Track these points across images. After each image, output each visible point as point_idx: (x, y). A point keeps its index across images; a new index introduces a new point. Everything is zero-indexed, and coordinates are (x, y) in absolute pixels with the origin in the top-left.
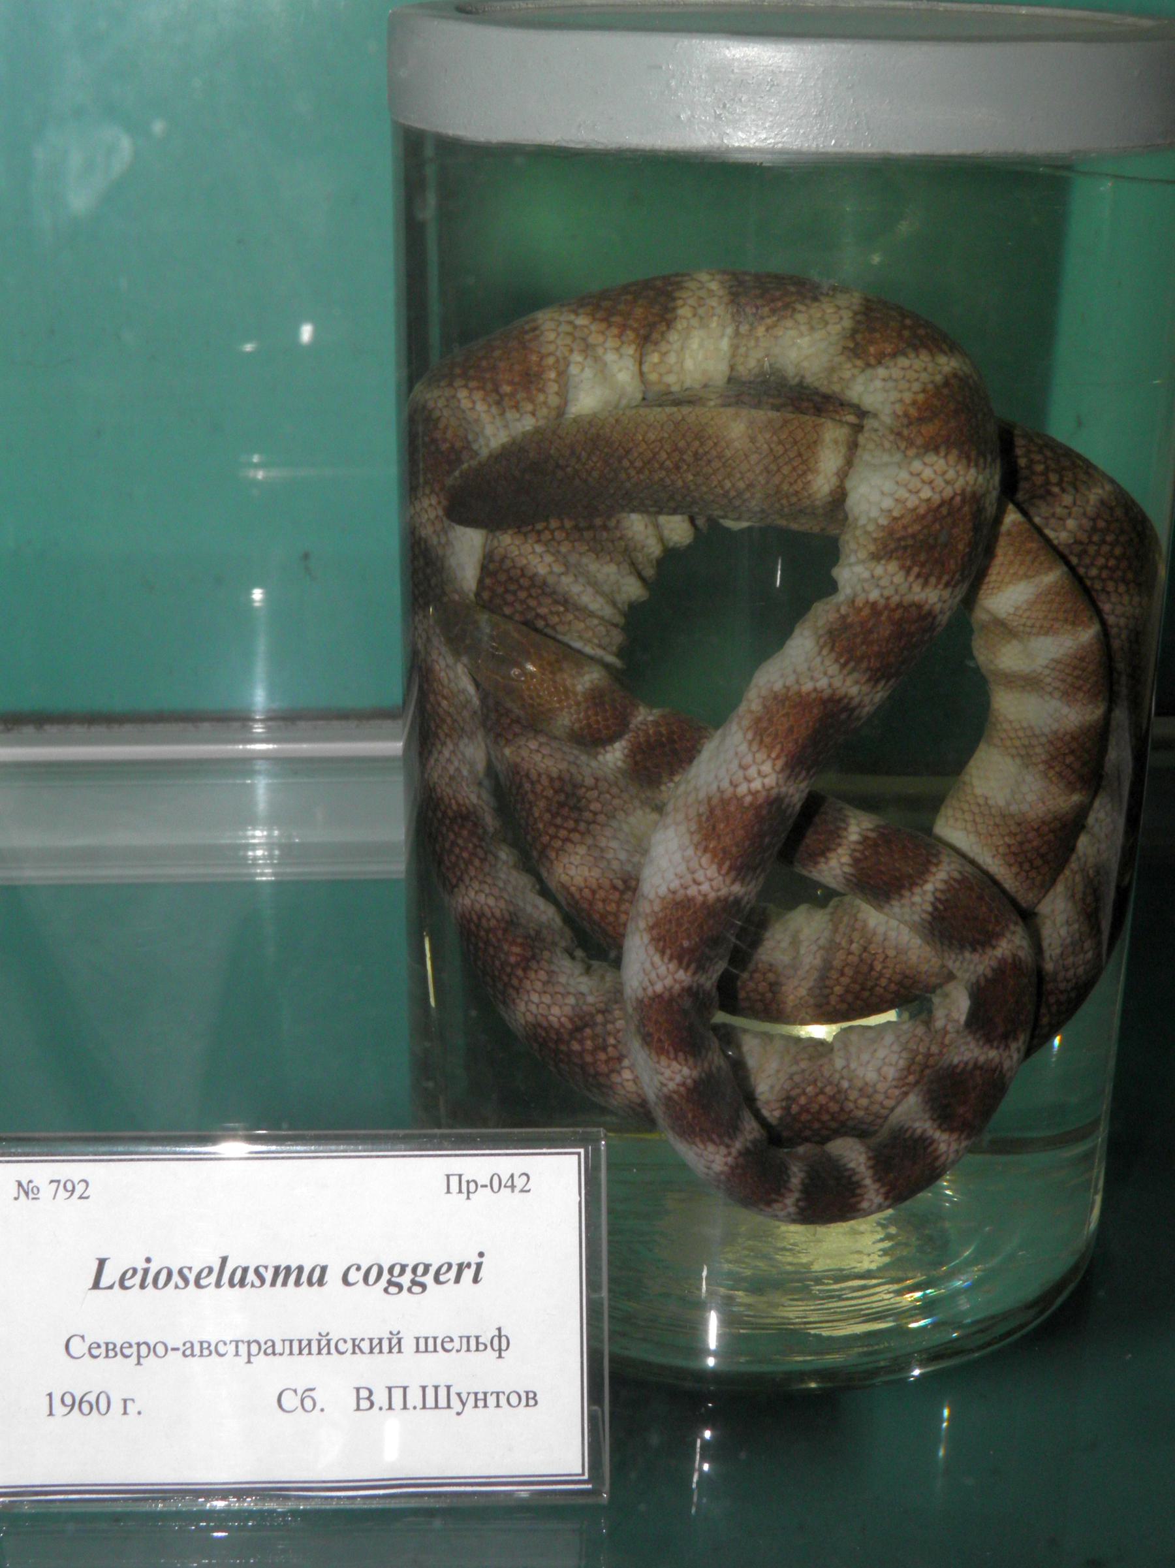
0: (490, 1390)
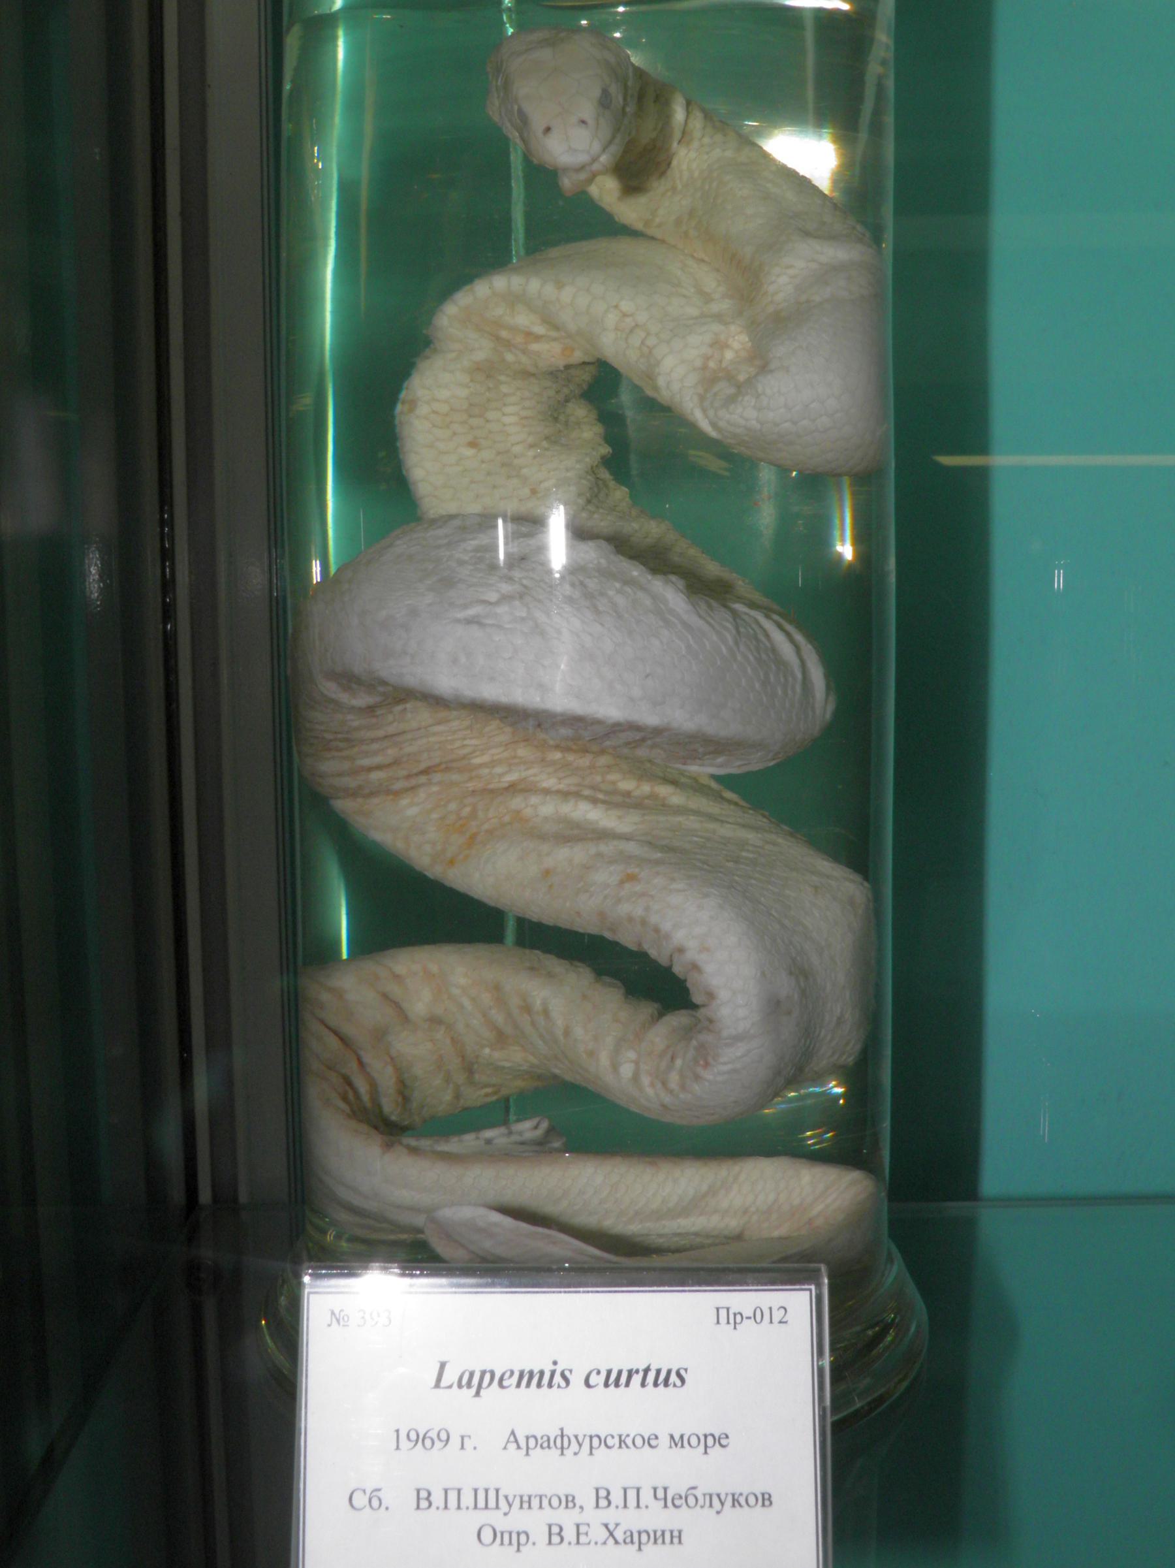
0: (534, 1493)
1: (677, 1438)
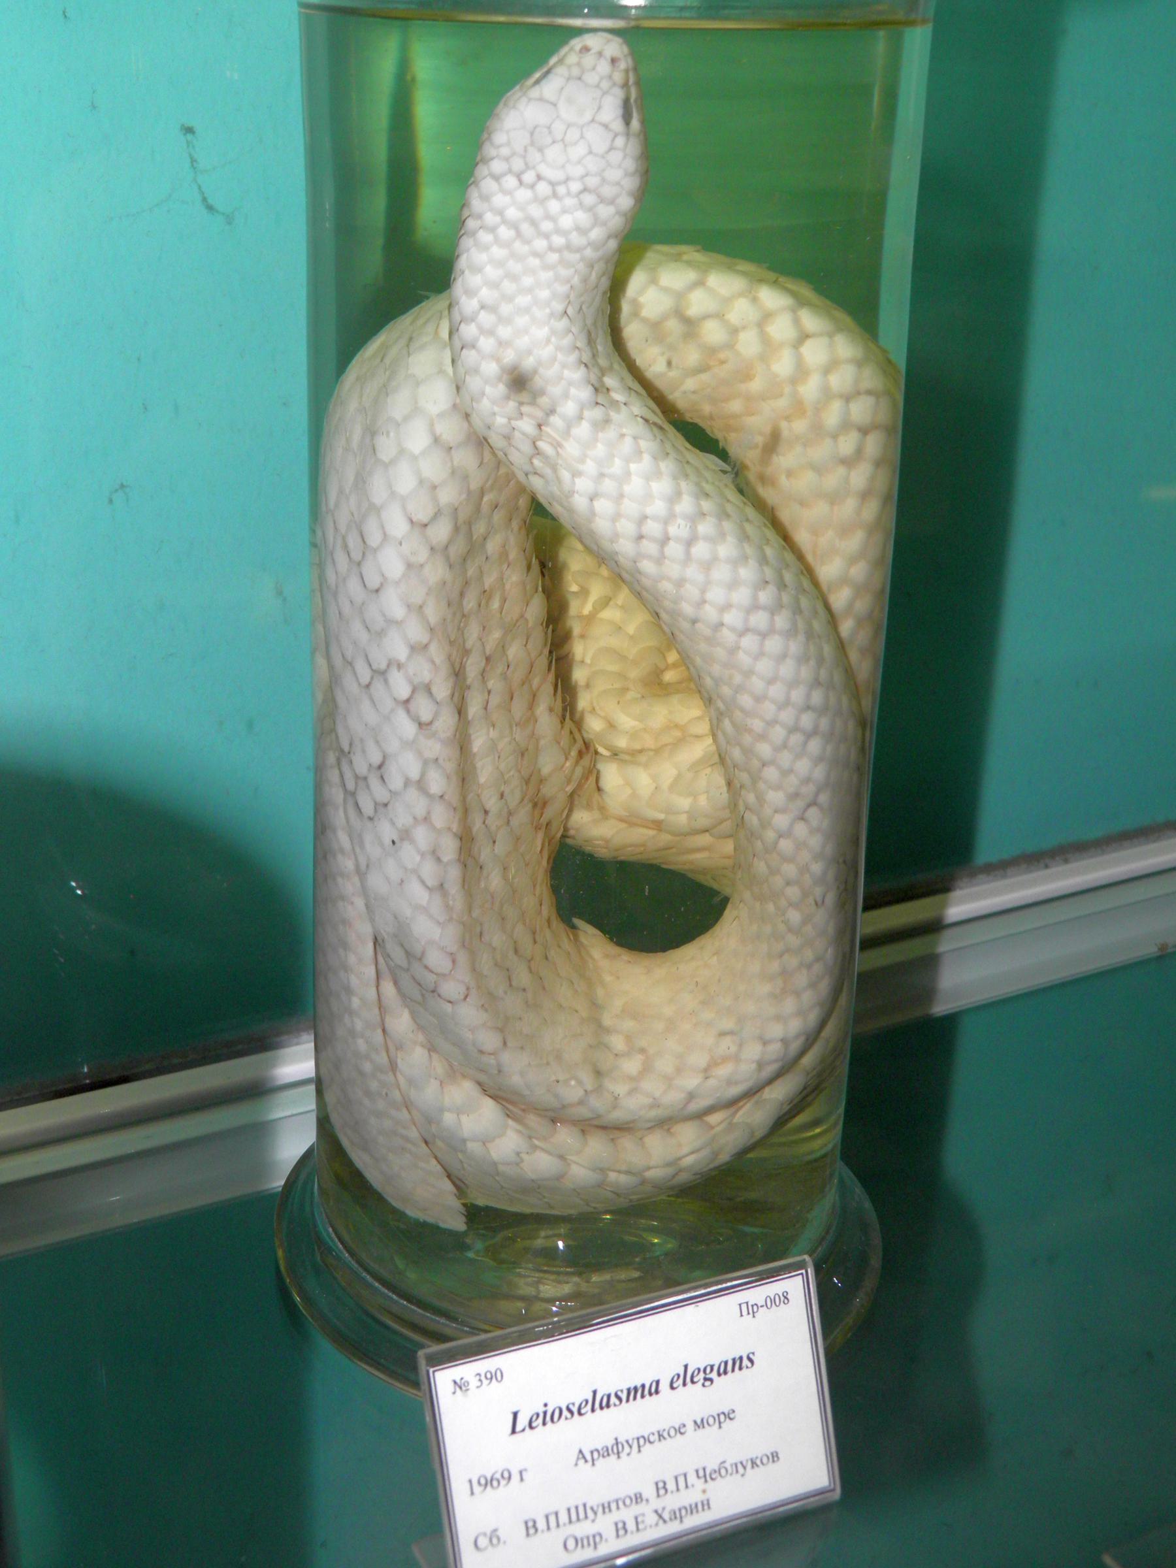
1: (699, 1421)
